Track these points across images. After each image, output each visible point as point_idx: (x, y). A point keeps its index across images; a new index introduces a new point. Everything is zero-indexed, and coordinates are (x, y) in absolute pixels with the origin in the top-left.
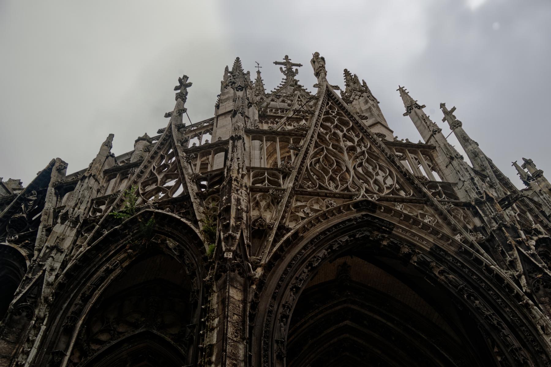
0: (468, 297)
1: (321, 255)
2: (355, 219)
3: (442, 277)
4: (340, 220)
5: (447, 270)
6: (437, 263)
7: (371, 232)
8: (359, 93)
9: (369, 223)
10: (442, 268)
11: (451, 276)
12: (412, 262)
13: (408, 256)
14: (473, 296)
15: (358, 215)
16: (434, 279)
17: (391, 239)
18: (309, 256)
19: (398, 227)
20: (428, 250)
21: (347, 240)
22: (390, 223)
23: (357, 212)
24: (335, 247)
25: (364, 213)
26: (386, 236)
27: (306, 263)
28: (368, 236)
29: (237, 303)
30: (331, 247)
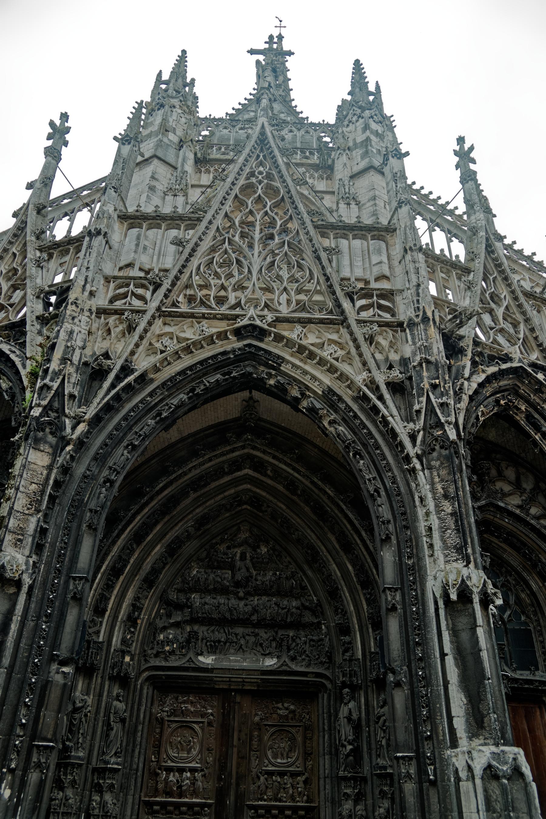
0: (354, 455)
1: (175, 401)
2: (233, 351)
3: (332, 429)
4: (210, 354)
5: (339, 419)
6: (328, 411)
7: (253, 366)
8: (359, 111)
9: (251, 355)
10: (332, 417)
11: (341, 428)
12: (300, 407)
13: (297, 400)
14: (360, 455)
15: (240, 344)
16: (324, 430)
17: (279, 378)
18: (156, 405)
19: (288, 362)
20: (320, 393)
21: (217, 380)
22: (279, 357)
23: (239, 340)
24: (198, 390)
25: (245, 342)
26: (274, 372)
27: (154, 413)
28: (251, 374)
29: (39, 470)
30: (193, 390)
